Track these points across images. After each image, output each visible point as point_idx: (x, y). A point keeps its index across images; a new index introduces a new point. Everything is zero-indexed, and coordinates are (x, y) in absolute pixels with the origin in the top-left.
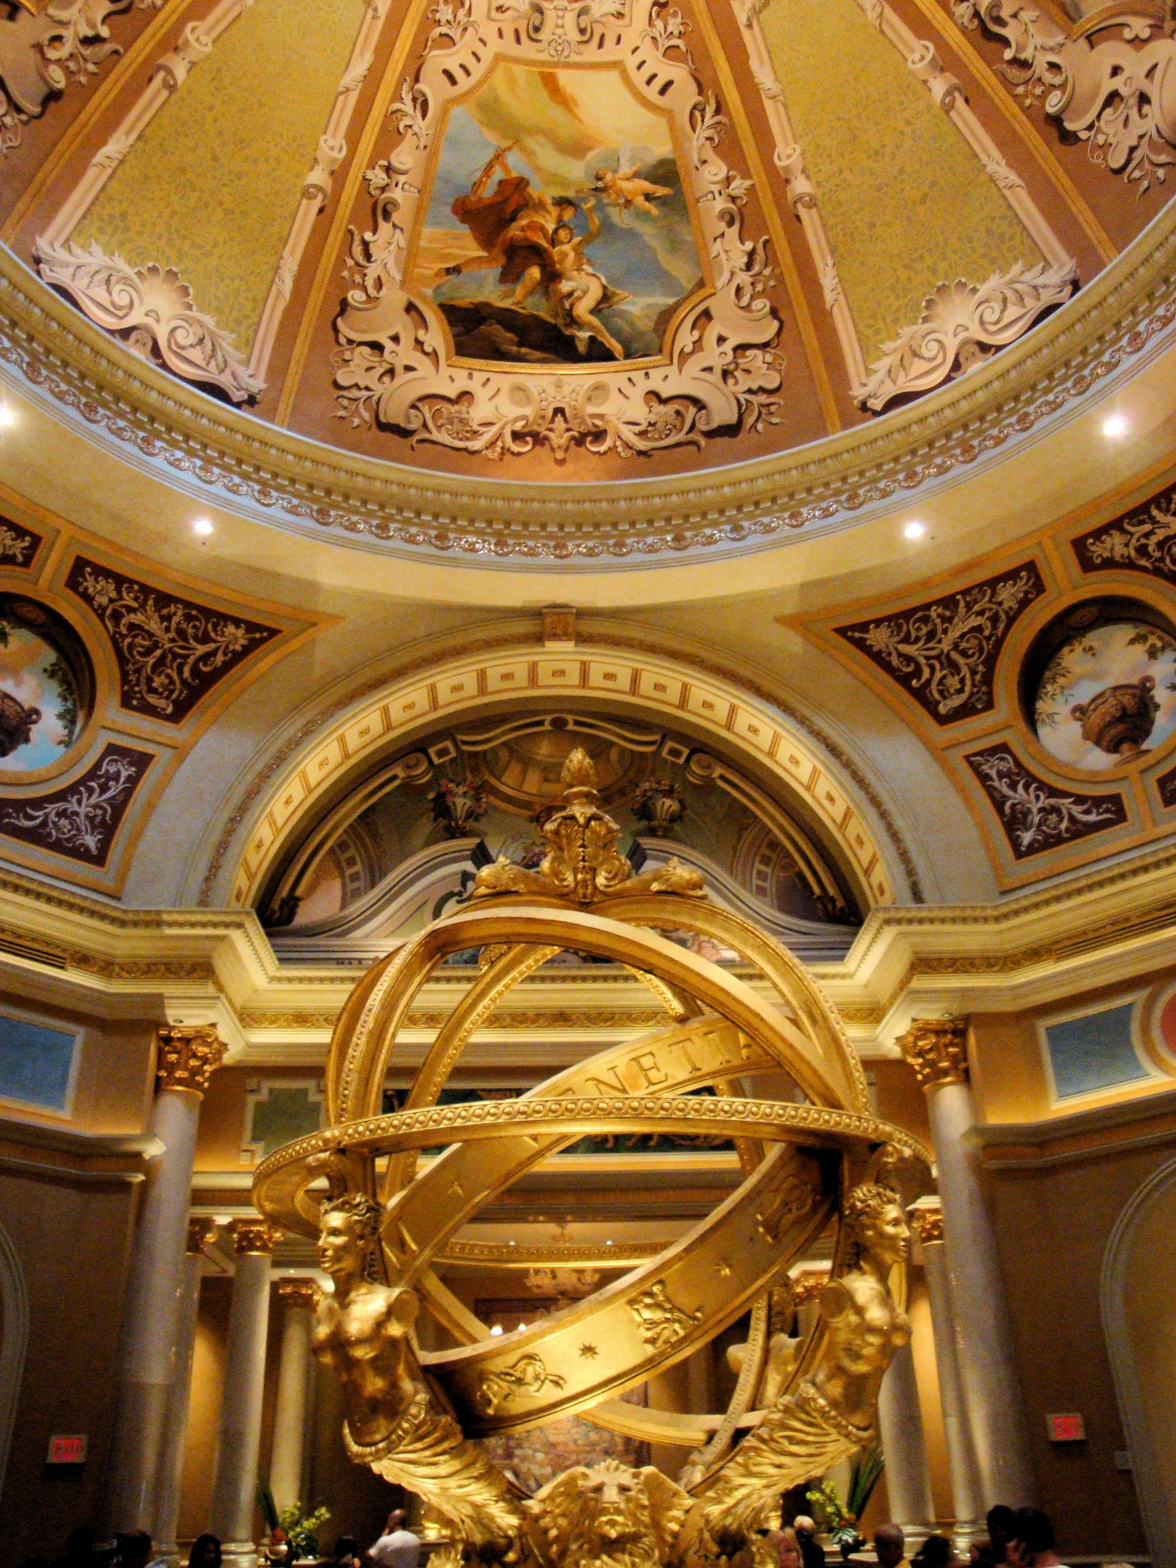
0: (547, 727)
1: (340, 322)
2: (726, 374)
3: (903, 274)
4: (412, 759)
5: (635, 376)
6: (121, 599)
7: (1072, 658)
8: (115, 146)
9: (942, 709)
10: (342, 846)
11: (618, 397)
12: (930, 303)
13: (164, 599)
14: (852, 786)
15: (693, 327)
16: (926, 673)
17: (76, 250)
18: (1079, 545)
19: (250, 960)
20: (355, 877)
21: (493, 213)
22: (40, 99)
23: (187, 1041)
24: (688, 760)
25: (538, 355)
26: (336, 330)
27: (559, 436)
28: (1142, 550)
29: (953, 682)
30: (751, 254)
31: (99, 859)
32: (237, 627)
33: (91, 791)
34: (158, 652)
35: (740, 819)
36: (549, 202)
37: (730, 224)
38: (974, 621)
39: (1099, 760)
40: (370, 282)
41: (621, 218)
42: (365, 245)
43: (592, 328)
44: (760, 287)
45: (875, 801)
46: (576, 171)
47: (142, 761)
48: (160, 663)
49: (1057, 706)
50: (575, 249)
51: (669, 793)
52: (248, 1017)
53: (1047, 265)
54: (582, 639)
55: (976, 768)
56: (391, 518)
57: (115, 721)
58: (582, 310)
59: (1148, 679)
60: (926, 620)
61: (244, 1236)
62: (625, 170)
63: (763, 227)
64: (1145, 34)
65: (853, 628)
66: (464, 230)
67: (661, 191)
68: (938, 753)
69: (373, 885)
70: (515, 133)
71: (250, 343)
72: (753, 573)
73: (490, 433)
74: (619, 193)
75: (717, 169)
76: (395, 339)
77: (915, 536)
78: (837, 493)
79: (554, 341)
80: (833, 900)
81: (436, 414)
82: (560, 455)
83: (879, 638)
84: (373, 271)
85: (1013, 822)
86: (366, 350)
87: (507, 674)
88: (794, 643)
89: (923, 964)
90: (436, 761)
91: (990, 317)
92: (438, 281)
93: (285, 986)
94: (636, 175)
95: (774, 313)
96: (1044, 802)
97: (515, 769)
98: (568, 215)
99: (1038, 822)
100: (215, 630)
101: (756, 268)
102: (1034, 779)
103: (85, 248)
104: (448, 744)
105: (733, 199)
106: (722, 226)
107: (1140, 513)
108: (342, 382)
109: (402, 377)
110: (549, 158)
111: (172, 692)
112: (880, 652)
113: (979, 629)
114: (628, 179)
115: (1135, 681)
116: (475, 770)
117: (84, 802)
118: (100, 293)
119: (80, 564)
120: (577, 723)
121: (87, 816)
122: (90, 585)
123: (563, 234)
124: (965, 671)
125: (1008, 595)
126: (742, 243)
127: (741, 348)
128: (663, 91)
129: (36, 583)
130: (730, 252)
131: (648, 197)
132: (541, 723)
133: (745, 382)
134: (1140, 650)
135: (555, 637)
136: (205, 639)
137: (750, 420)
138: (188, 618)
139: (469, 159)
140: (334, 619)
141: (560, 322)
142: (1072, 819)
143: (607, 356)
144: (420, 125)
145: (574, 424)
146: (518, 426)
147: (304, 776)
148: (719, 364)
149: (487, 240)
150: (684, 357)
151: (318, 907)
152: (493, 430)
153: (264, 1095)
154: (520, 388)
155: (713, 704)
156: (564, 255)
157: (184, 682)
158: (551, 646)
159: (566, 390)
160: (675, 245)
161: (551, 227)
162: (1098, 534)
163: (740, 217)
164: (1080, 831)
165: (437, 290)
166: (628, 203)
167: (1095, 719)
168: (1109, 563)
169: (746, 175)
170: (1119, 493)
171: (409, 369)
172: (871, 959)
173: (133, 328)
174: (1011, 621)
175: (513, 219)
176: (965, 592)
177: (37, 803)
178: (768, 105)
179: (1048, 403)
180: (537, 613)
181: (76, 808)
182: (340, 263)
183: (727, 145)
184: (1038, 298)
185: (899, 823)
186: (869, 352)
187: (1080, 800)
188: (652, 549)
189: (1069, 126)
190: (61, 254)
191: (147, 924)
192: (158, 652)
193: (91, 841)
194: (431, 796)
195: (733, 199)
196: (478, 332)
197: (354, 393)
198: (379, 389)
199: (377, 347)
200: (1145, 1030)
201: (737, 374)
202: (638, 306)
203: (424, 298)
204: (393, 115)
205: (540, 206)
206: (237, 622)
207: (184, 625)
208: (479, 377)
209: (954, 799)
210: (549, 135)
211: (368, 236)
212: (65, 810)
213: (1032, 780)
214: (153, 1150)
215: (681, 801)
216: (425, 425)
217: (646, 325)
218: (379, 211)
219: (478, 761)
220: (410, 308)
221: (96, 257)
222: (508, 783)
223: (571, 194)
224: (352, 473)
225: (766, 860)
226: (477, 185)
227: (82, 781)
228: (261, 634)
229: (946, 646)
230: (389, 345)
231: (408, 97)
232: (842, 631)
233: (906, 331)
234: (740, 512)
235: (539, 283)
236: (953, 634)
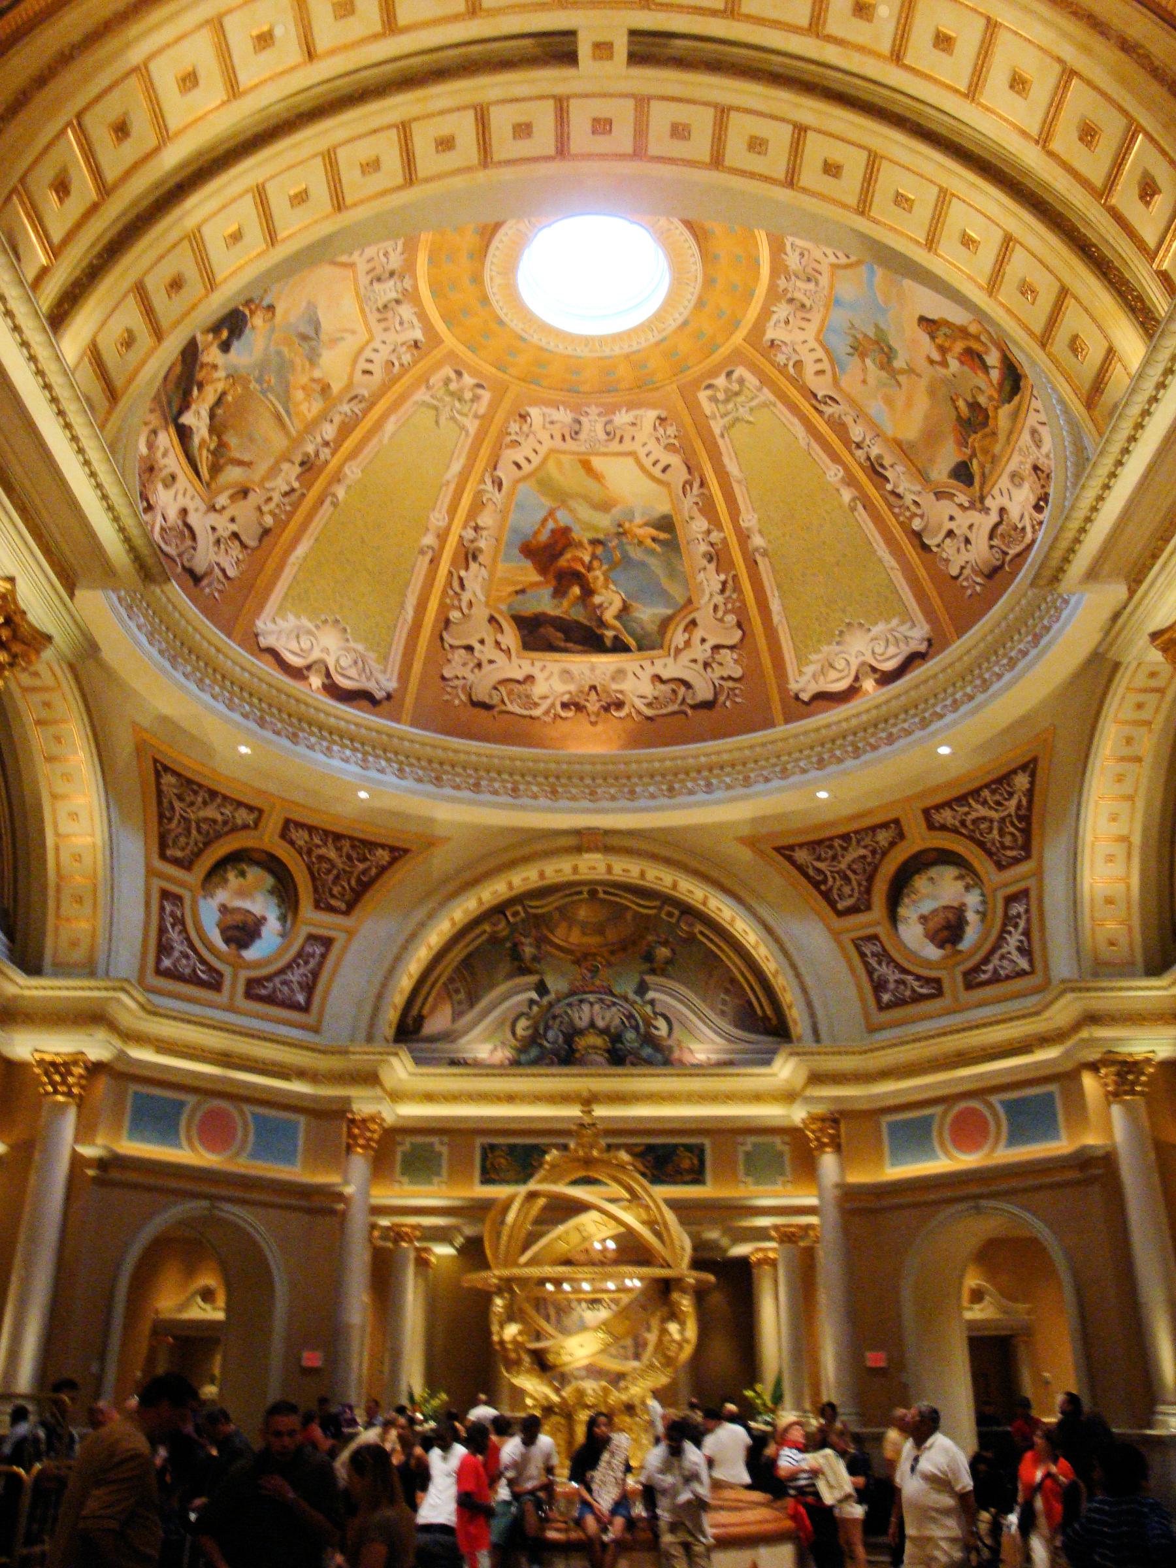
0: (585, 895)
1: (445, 635)
2: (706, 665)
3: (824, 610)
4: (495, 919)
5: (644, 663)
7: (920, 883)
8: (301, 551)
9: (840, 906)
10: (451, 980)
11: (634, 678)
12: (841, 632)
13: (338, 837)
14: (781, 958)
15: (685, 630)
16: (830, 880)
17: (278, 620)
18: (926, 812)
19: (400, 1069)
20: (460, 1003)
21: (549, 554)
22: (257, 537)
23: (364, 1121)
24: (678, 921)
25: (580, 648)
26: (442, 639)
27: (593, 705)
28: (963, 823)
29: (847, 890)
30: (724, 583)
31: (305, 1009)
33: (298, 965)
34: (335, 872)
35: (711, 961)
36: (585, 541)
37: (710, 561)
38: (862, 852)
39: (932, 952)
40: (464, 605)
41: (636, 554)
42: (461, 579)
43: (614, 628)
44: (730, 606)
45: (794, 967)
46: (604, 521)
47: (327, 942)
48: (337, 877)
49: (910, 912)
50: (604, 574)
51: (665, 943)
52: (396, 1096)
53: (913, 625)
54: (608, 849)
55: (857, 947)
56: (481, 778)
57: (312, 919)
58: (609, 616)
59: (964, 905)
60: (831, 847)
61: (398, 1234)
62: (638, 520)
63: (732, 565)
64: (967, 504)
65: (784, 848)
66: (528, 564)
67: (663, 536)
68: (836, 935)
69: (472, 1005)
70: (562, 497)
71: (385, 658)
72: (722, 812)
73: (545, 705)
74: (635, 535)
75: (700, 524)
76: (482, 642)
77: (824, 796)
78: (775, 765)
79: (589, 638)
80: (769, 1019)
81: (510, 693)
82: (593, 719)
83: (802, 856)
84: (466, 597)
85: (879, 986)
86: (462, 651)
87: (559, 869)
89: (816, 1078)
90: (511, 919)
91: (879, 650)
92: (509, 600)
93: (419, 1078)
94: (646, 524)
95: (739, 625)
96: (898, 976)
97: (564, 926)
98: (599, 550)
99: (894, 990)
101: (727, 593)
102: (893, 961)
103: (285, 619)
104: (519, 908)
105: (712, 545)
106: (704, 562)
107: (961, 799)
108: (447, 674)
109: (487, 668)
110: (585, 513)
113: (864, 857)
114: (640, 527)
115: (955, 904)
116: (537, 926)
118: (294, 645)
119: (287, 822)
120: (605, 892)
122: (295, 834)
123: (596, 564)
124: (854, 883)
125: (883, 837)
126: (718, 573)
127: (716, 648)
128: (664, 470)
129: (261, 839)
130: (710, 580)
131: (654, 539)
132: (580, 893)
133: (719, 672)
134: (960, 885)
135: (589, 850)
136: (365, 859)
137: (722, 698)
139: (532, 515)
140: (448, 839)
141: (593, 624)
142: (913, 991)
143: (626, 649)
144: (498, 497)
145: (603, 696)
146: (566, 698)
148: (701, 657)
149: (543, 570)
150: (678, 651)
151: (438, 1021)
152: (549, 702)
153: (407, 1146)
154: (567, 672)
155: (693, 891)
156: (596, 578)
157: (351, 888)
158: (586, 856)
159: (598, 672)
160: (672, 573)
161: (587, 559)
162: (938, 807)
163: (718, 557)
164: (918, 998)
165: (510, 606)
166: (640, 543)
167: (931, 924)
168: (943, 828)
169: (720, 528)
170: (949, 785)
171: (491, 662)
172: (785, 1070)
173: (315, 662)
174: (884, 854)
175: (561, 554)
176: (856, 832)
177: (269, 978)
178: (735, 486)
179: (904, 730)
180: (578, 832)
182: (444, 593)
183: (707, 508)
184: (907, 644)
185: (809, 980)
186: (801, 660)
187: (918, 978)
188: (653, 796)
189: (926, 541)
190: (271, 626)
193: (301, 998)
194: (508, 945)
195: (712, 545)
196: (537, 633)
197: (456, 682)
198: (471, 677)
199: (469, 648)
200: (941, 1134)
201: (714, 665)
202: (647, 614)
203: (501, 612)
204: (480, 493)
205: (580, 545)
206: (383, 846)
208: (538, 664)
209: (843, 967)
210: (586, 498)
211: (463, 573)
213: (891, 960)
214: (349, 1190)
215: (673, 951)
216: (503, 701)
217: (652, 628)
218: (468, 555)
219: (539, 921)
220: (492, 619)
221: (290, 622)
222: (560, 935)
223: (601, 536)
224: (456, 751)
225: (727, 991)
226: (536, 533)
227: (294, 960)
228: (398, 853)
229: (843, 866)
230: (477, 646)
231: (488, 481)
232: (778, 850)
233: (826, 649)
234: (708, 776)
235: (578, 598)
236: (849, 858)
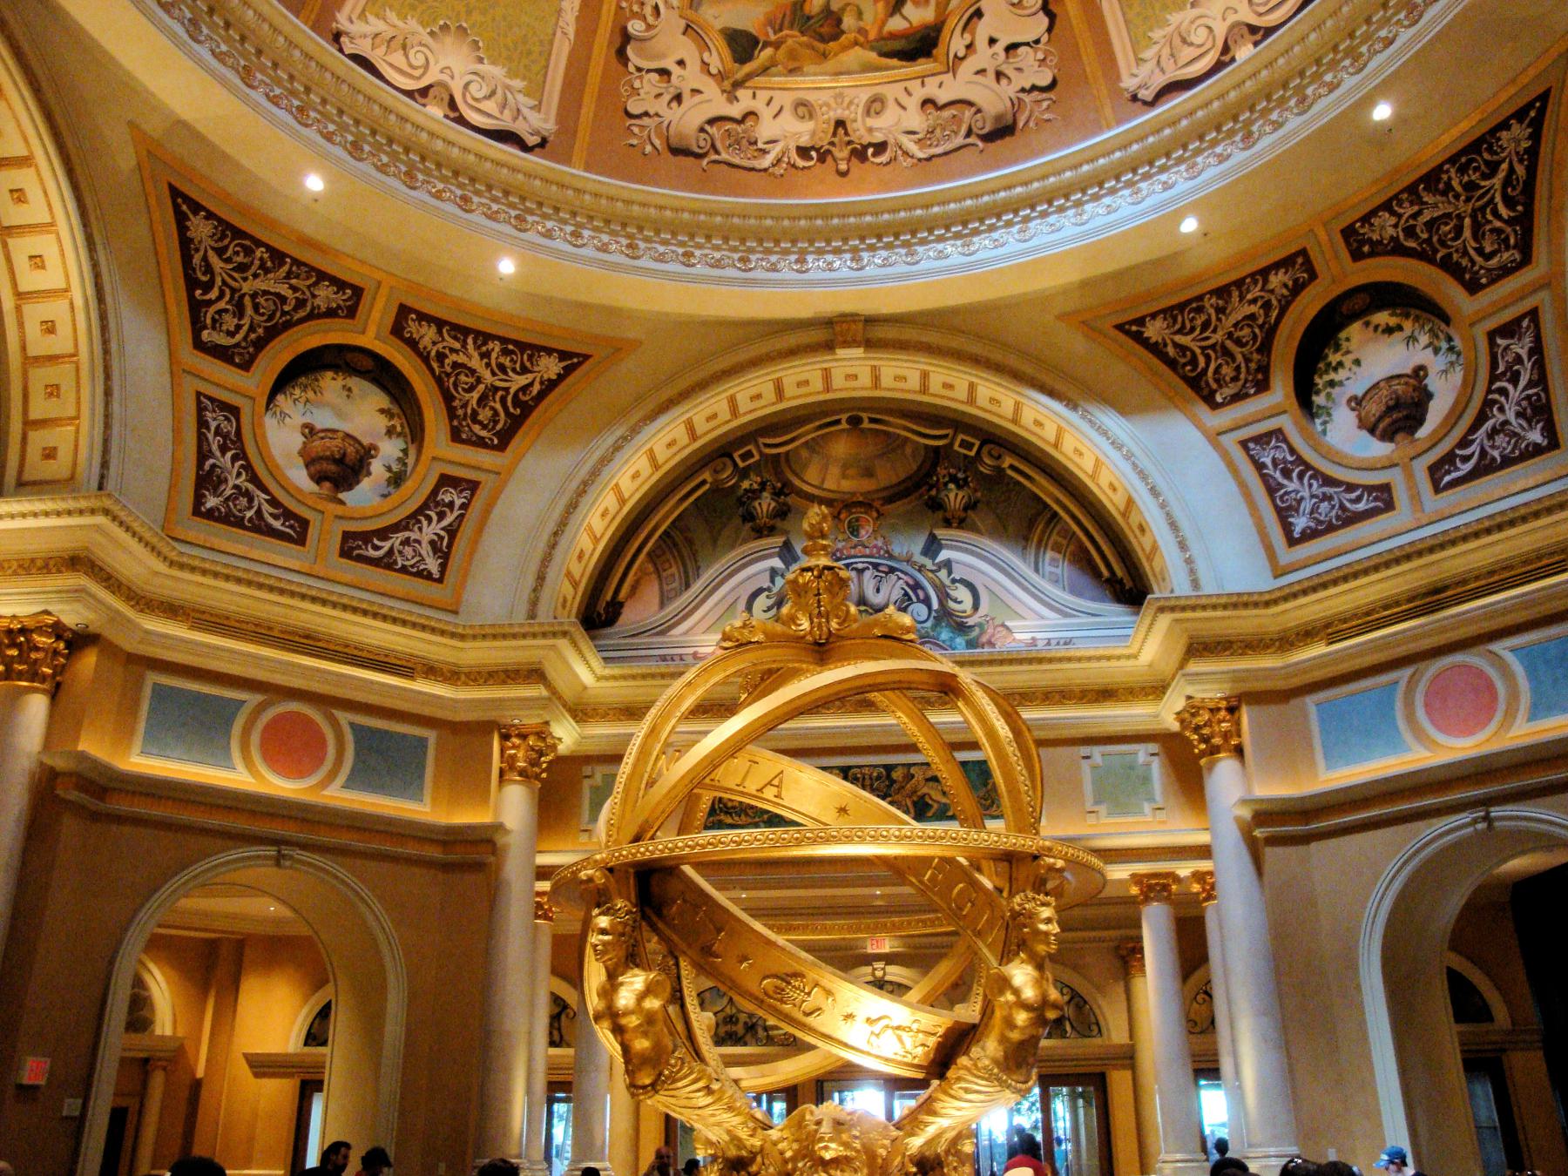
6: (1400, 216)
33: (1503, 392)
88: (126, 159)
121: (1519, 415)
181: (1501, 418)
192: (1467, 221)
193: (1535, 436)
212: (1494, 428)
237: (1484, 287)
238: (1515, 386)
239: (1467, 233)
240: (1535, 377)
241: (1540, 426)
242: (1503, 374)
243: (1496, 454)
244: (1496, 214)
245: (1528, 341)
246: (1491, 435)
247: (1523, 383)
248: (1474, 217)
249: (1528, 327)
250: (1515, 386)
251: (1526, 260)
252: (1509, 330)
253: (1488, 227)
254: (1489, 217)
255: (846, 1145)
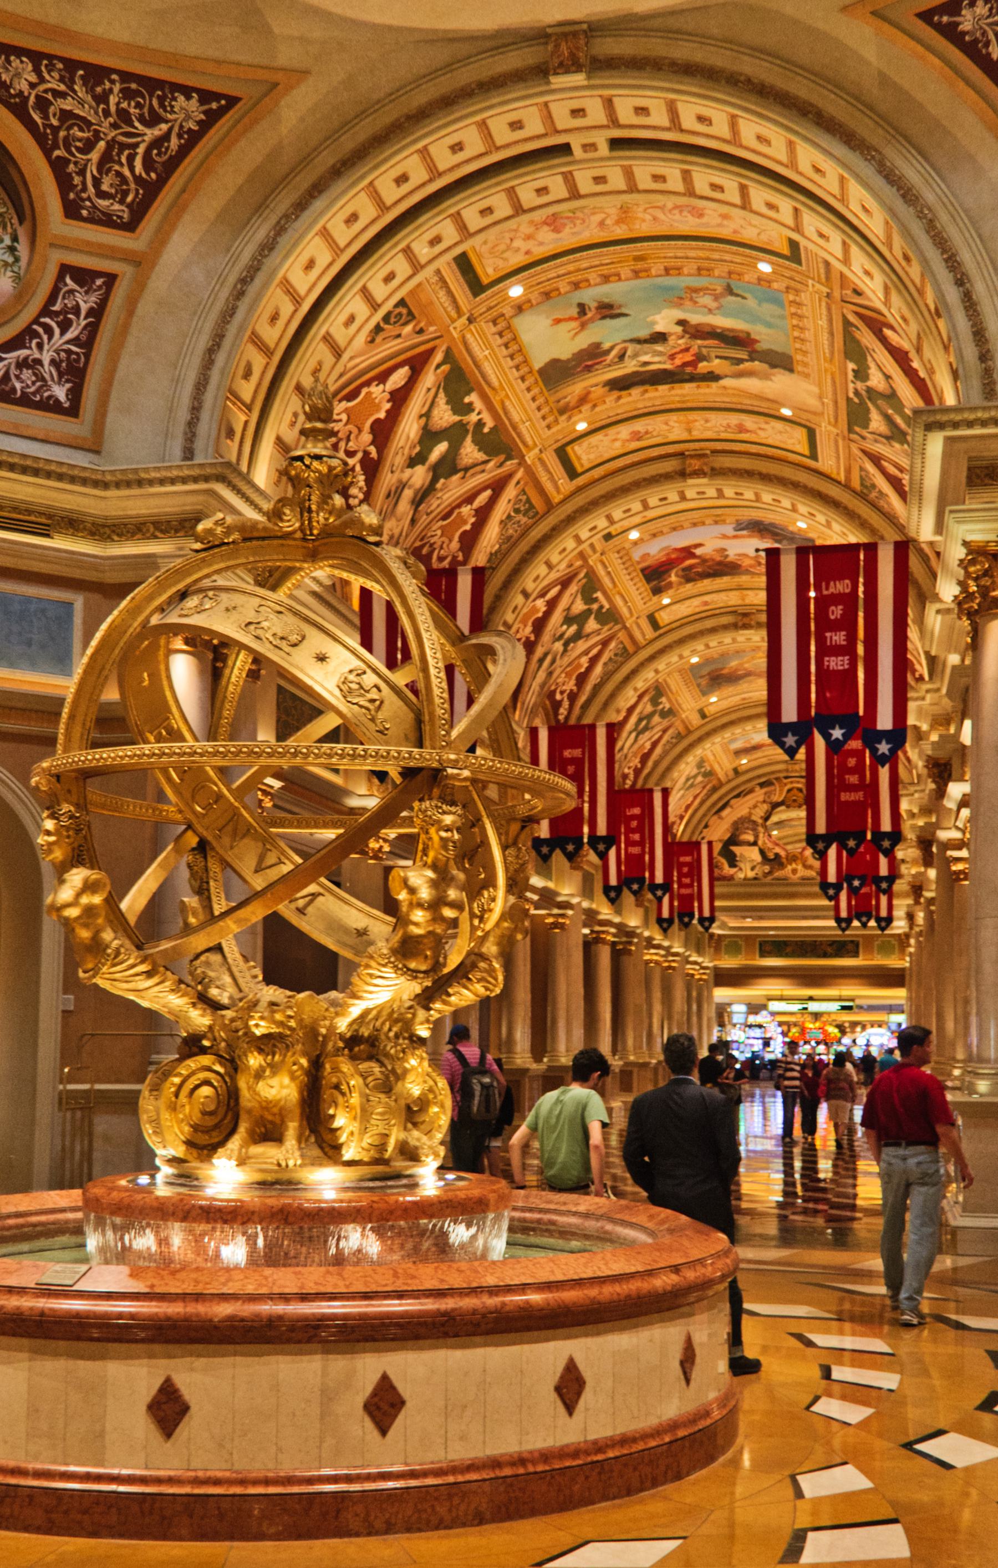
6: (42, 80)
13: (96, 74)
31: (73, 410)
32: (188, 98)
33: (49, 331)
100: (162, 105)
111: (125, 193)
112: (976, 41)
117: (46, 347)
121: (53, 362)
136: (153, 120)
138: (127, 94)
147: (289, 289)
157: (138, 179)
181: (37, 355)
191: (128, 484)
192: (102, 144)
193: (60, 392)
206: (187, 91)
207: (124, 105)
212: (26, 359)
237: (80, 218)
238: (63, 333)
239: (95, 156)
240: (84, 338)
241: (68, 385)
242: (57, 314)
243: (18, 386)
244: (131, 159)
245: (93, 299)
246: (23, 364)
247: (70, 335)
248: (110, 145)
249: (100, 287)
250: (63, 333)
251: (130, 226)
252: (84, 277)
253: (117, 167)
254: (124, 160)
255: (281, 1024)
